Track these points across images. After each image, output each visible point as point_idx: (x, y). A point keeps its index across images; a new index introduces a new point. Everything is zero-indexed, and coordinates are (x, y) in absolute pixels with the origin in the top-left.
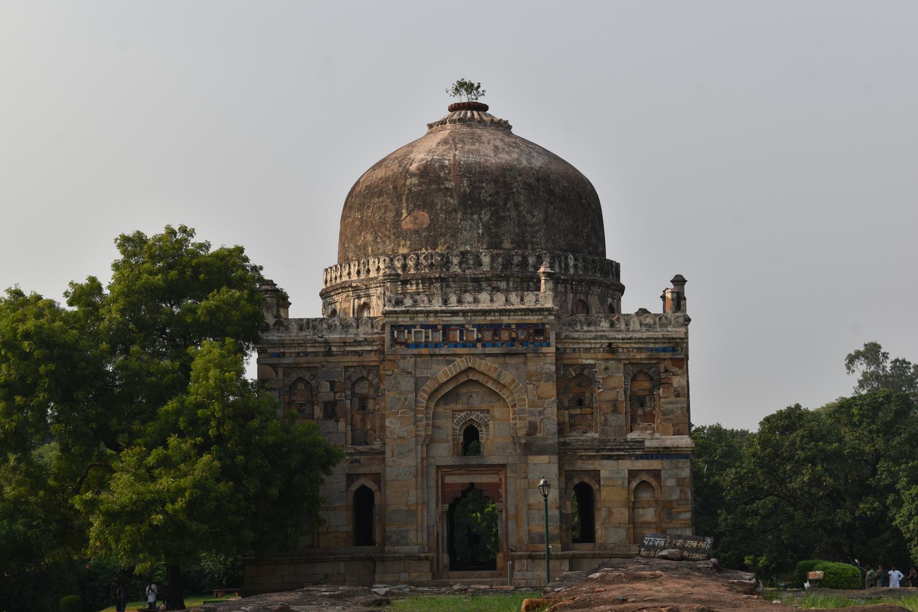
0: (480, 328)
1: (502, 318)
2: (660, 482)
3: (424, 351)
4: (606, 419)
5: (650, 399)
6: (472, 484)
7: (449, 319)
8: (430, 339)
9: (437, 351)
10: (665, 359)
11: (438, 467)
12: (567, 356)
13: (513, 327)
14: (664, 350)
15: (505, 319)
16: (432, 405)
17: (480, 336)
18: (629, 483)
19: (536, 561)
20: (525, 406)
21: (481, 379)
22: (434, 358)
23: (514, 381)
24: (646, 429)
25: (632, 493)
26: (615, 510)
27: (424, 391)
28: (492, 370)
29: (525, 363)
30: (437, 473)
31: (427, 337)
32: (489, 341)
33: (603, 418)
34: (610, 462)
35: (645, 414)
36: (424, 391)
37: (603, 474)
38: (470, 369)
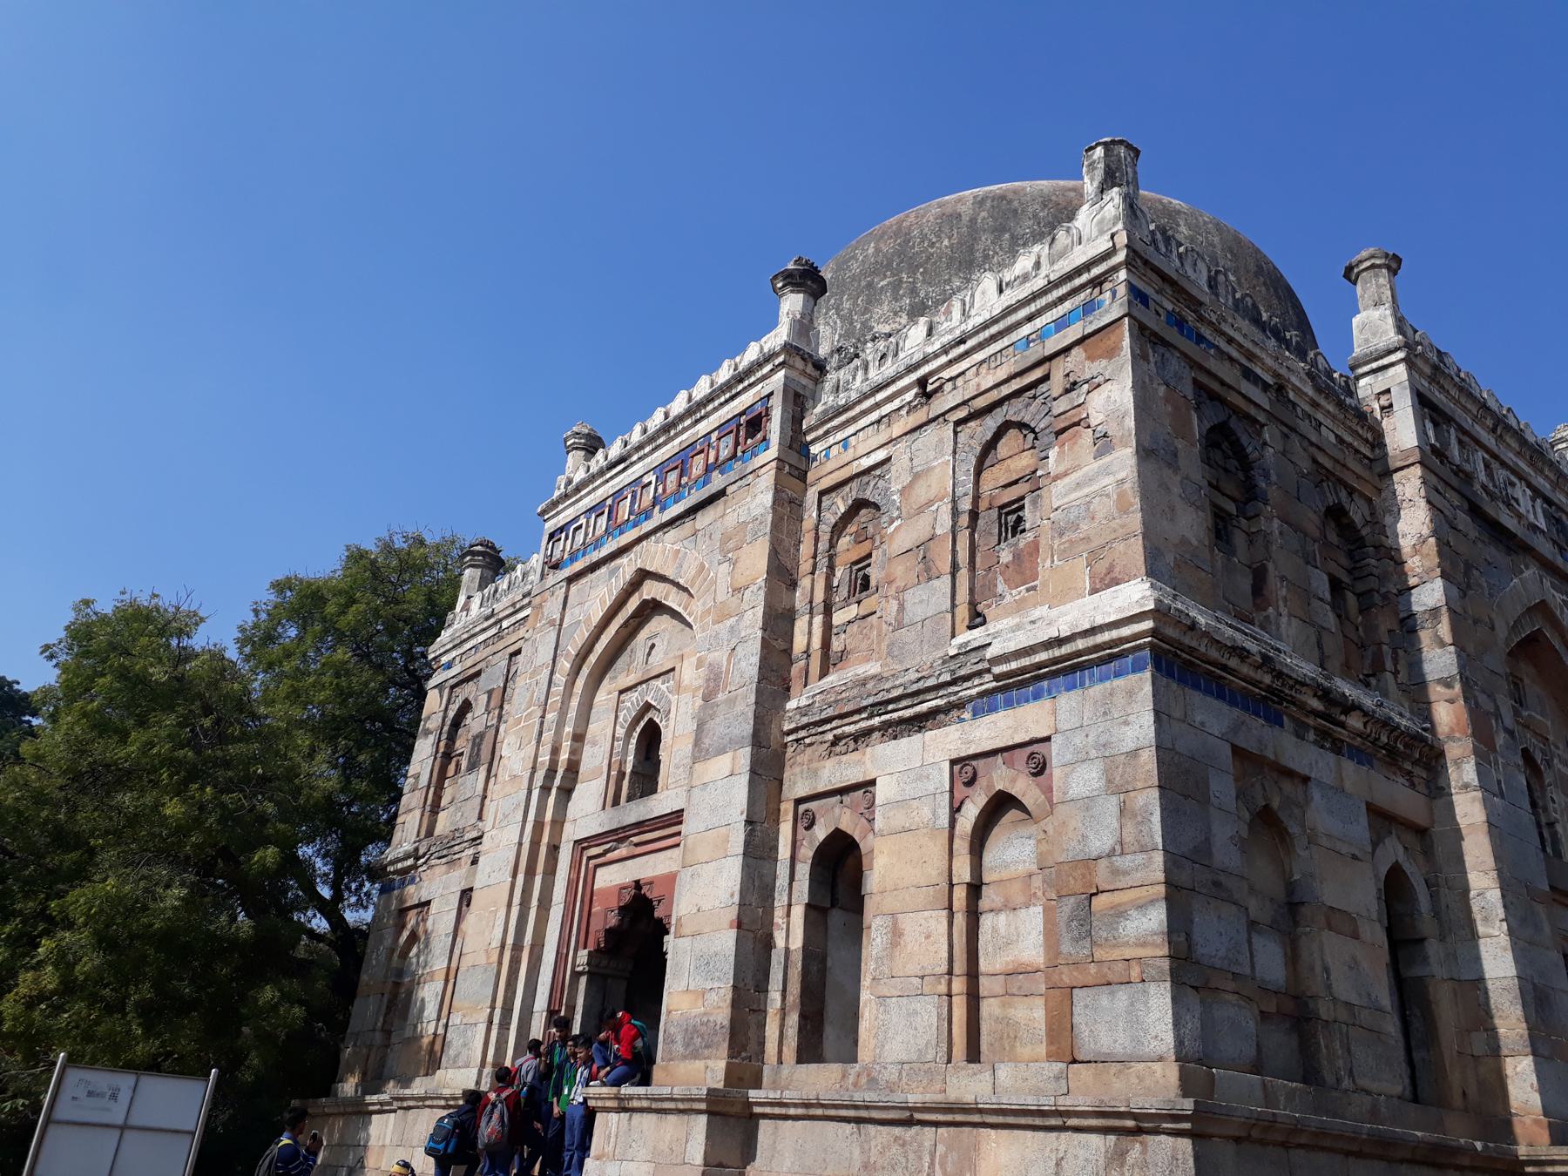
0: (662, 470)
2: (1048, 791)
4: (901, 608)
5: (1034, 502)
6: (637, 884)
10: (1066, 350)
11: (581, 844)
12: (830, 466)
14: (1061, 324)
18: (955, 810)
19: (637, 1117)
23: (702, 566)
24: (1020, 606)
25: (962, 846)
26: (908, 923)
30: (575, 864)
31: (586, 534)
33: (894, 605)
34: (909, 746)
35: (1017, 557)
37: (882, 792)
38: (643, 575)
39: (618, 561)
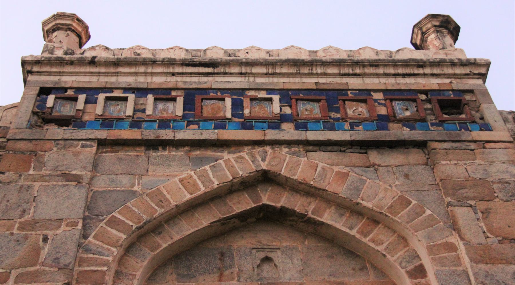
1: (345, 80)
3: (127, 134)
7: (205, 79)
8: (149, 112)
9: (167, 134)
13: (379, 96)
15: (354, 83)
16: (140, 266)
17: (287, 110)
20: (458, 261)
21: (298, 204)
22: (152, 153)
23: (404, 202)
27: (114, 223)
28: (330, 177)
29: (431, 164)
32: (317, 121)
36: (114, 223)
39: (210, 153)
